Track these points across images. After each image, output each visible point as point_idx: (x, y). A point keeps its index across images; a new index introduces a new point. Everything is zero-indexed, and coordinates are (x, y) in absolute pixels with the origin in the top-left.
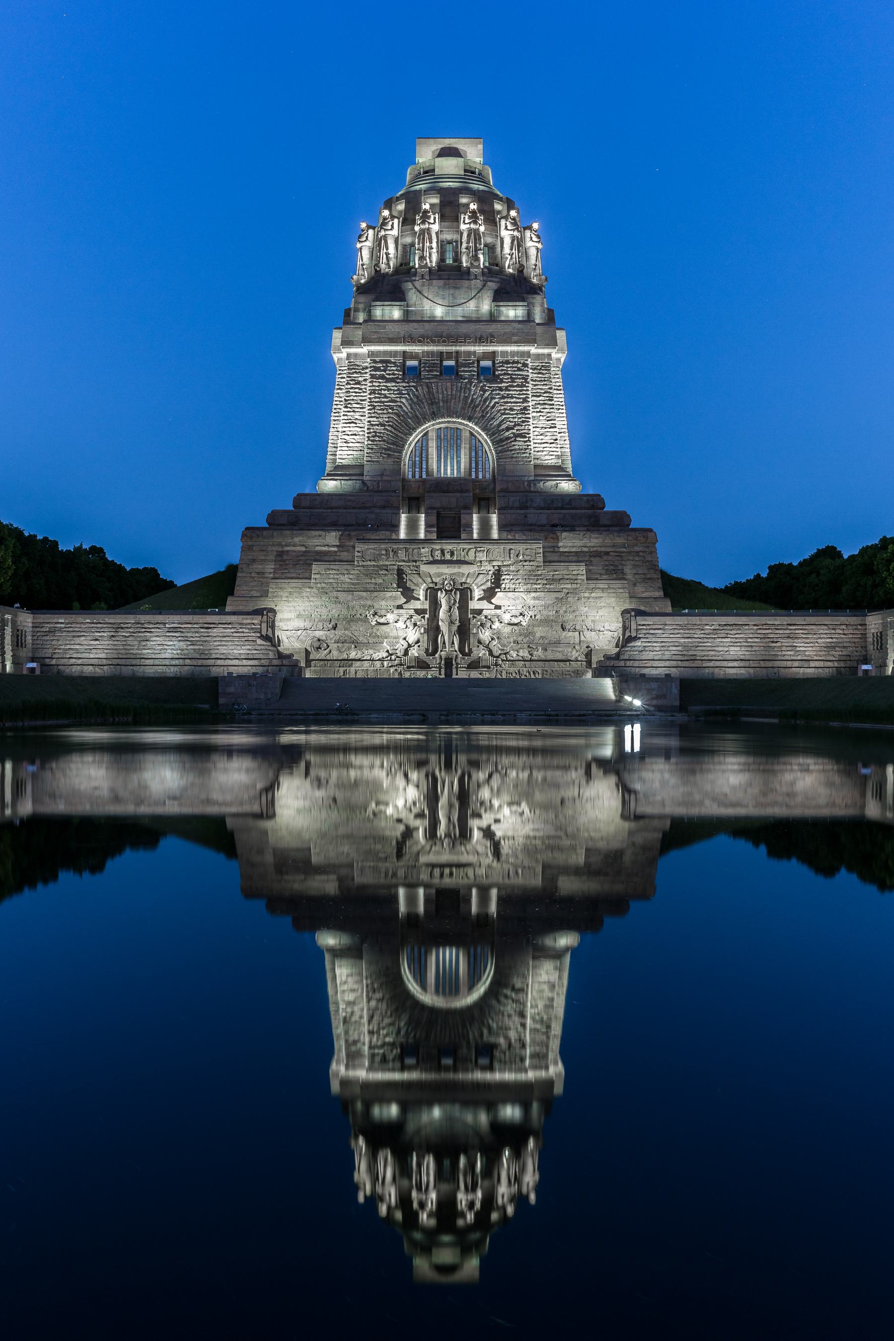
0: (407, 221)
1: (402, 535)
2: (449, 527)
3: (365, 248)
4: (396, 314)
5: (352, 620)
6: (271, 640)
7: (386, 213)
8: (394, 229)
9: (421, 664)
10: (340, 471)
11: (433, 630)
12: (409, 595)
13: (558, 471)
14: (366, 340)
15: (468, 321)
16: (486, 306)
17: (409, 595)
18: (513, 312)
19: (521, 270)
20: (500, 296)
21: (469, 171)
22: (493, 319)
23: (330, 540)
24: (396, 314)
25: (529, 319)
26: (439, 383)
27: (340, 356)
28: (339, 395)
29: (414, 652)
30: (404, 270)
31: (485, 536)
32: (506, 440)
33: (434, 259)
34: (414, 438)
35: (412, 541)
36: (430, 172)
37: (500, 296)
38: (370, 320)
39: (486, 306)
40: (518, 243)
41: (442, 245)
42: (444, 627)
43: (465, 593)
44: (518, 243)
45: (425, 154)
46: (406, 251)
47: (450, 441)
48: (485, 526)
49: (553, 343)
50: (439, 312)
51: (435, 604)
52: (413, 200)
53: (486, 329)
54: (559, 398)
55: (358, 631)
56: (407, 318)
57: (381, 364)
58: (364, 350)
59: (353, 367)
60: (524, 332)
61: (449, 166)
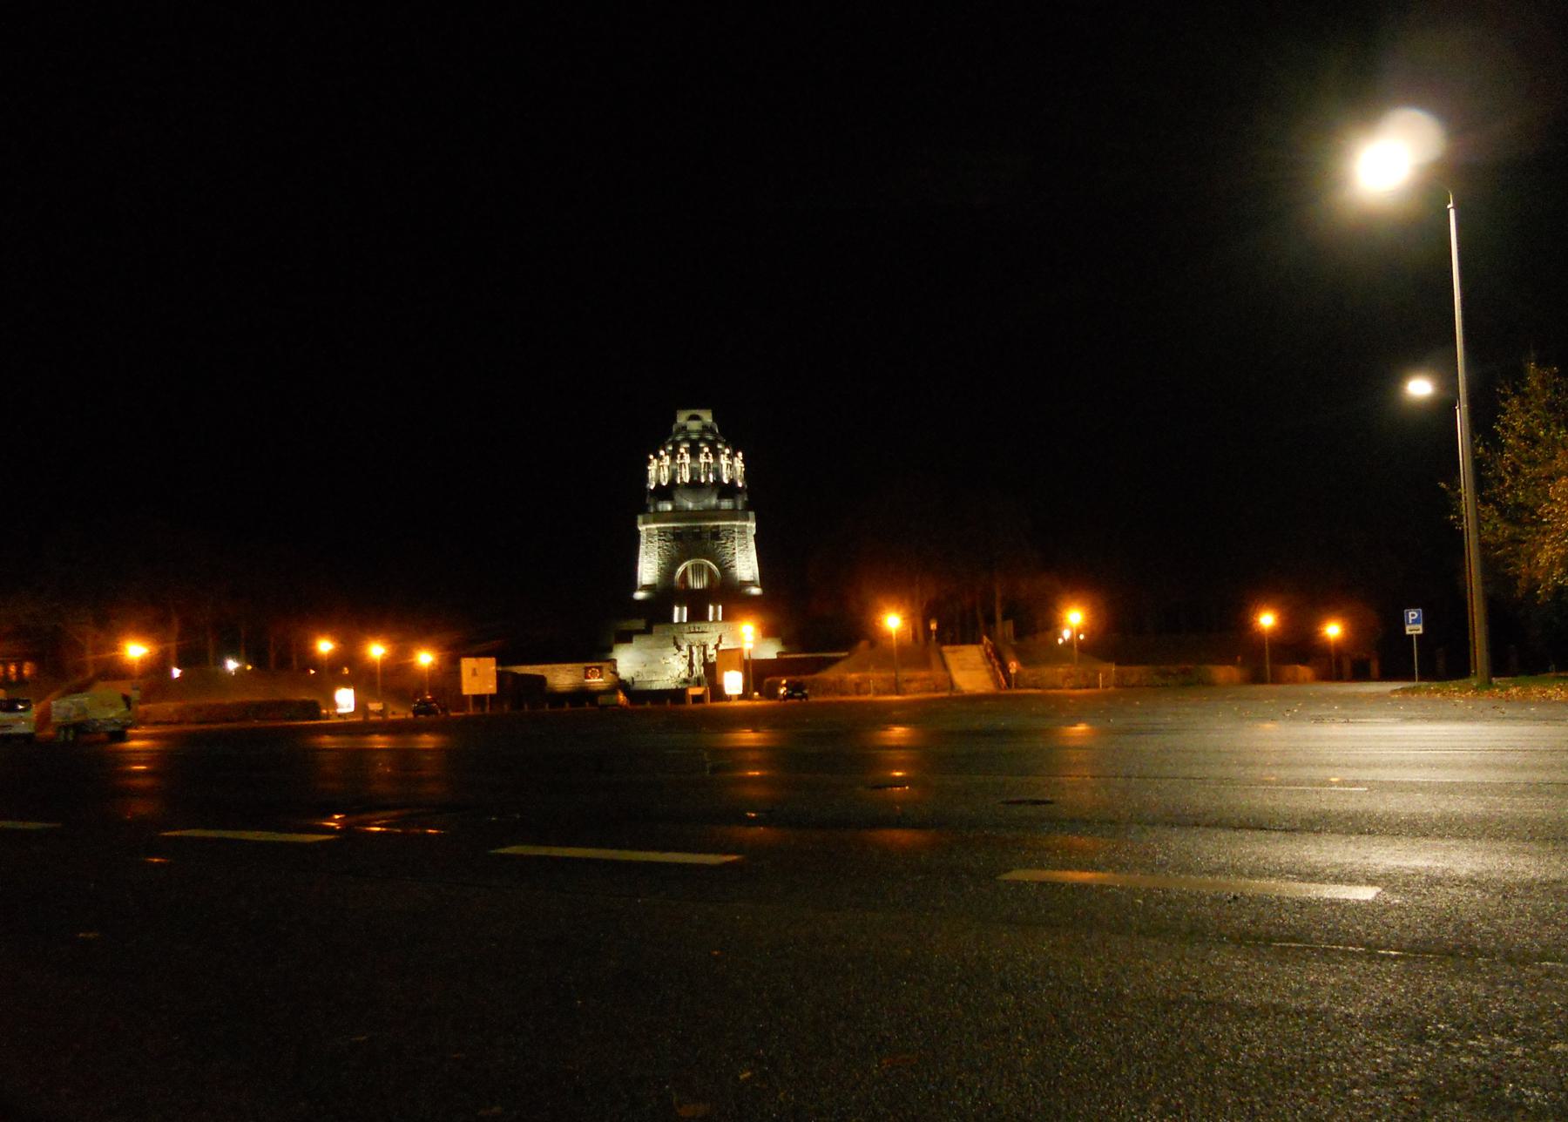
0: (673, 458)
1: (676, 620)
2: (698, 615)
3: (652, 468)
4: (669, 507)
5: (653, 662)
6: (615, 673)
7: (662, 453)
8: (667, 459)
9: (685, 681)
10: (645, 588)
11: (691, 665)
12: (679, 648)
13: (752, 583)
14: (655, 521)
15: (705, 510)
16: (714, 501)
17: (679, 648)
18: (726, 504)
19: (732, 482)
20: (720, 497)
21: (706, 429)
22: (717, 508)
23: (640, 624)
24: (669, 507)
25: (735, 509)
26: (694, 541)
27: (642, 528)
28: (642, 548)
29: (684, 676)
30: (672, 482)
31: (715, 620)
32: (726, 569)
33: (687, 479)
34: (680, 570)
35: (681, 623)
36: (684, 428)
37: (720, 497)
38: (657, 511)
39: (714, 501)
40: (731, 466)
41: (693, 472)
42: (695, 662)
43: (705, 647)
44: (731, 466)
45: (682, 418)
46: (673, 474)
47: (698, 570)
48: (716, 613)
49: (747, 519)
50: (690, 505)
51: (691, 653)
52: (676, 446)
53: (716, 513)
54: (752, 545)
55: (656, 667)
56: (674, 510)
57: (662, 532)
58: (654, 526)
59: (649, 535)
60: (732, 514)
61: (694, 426)
